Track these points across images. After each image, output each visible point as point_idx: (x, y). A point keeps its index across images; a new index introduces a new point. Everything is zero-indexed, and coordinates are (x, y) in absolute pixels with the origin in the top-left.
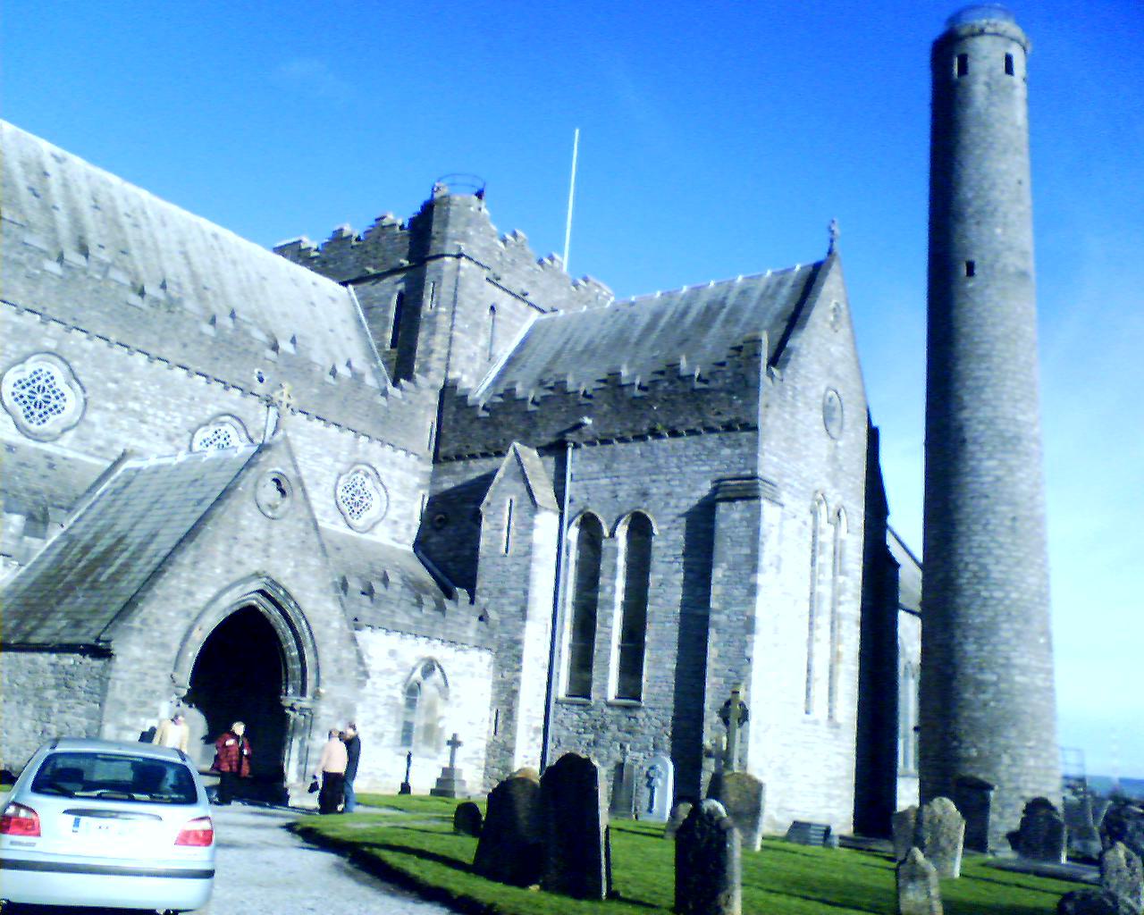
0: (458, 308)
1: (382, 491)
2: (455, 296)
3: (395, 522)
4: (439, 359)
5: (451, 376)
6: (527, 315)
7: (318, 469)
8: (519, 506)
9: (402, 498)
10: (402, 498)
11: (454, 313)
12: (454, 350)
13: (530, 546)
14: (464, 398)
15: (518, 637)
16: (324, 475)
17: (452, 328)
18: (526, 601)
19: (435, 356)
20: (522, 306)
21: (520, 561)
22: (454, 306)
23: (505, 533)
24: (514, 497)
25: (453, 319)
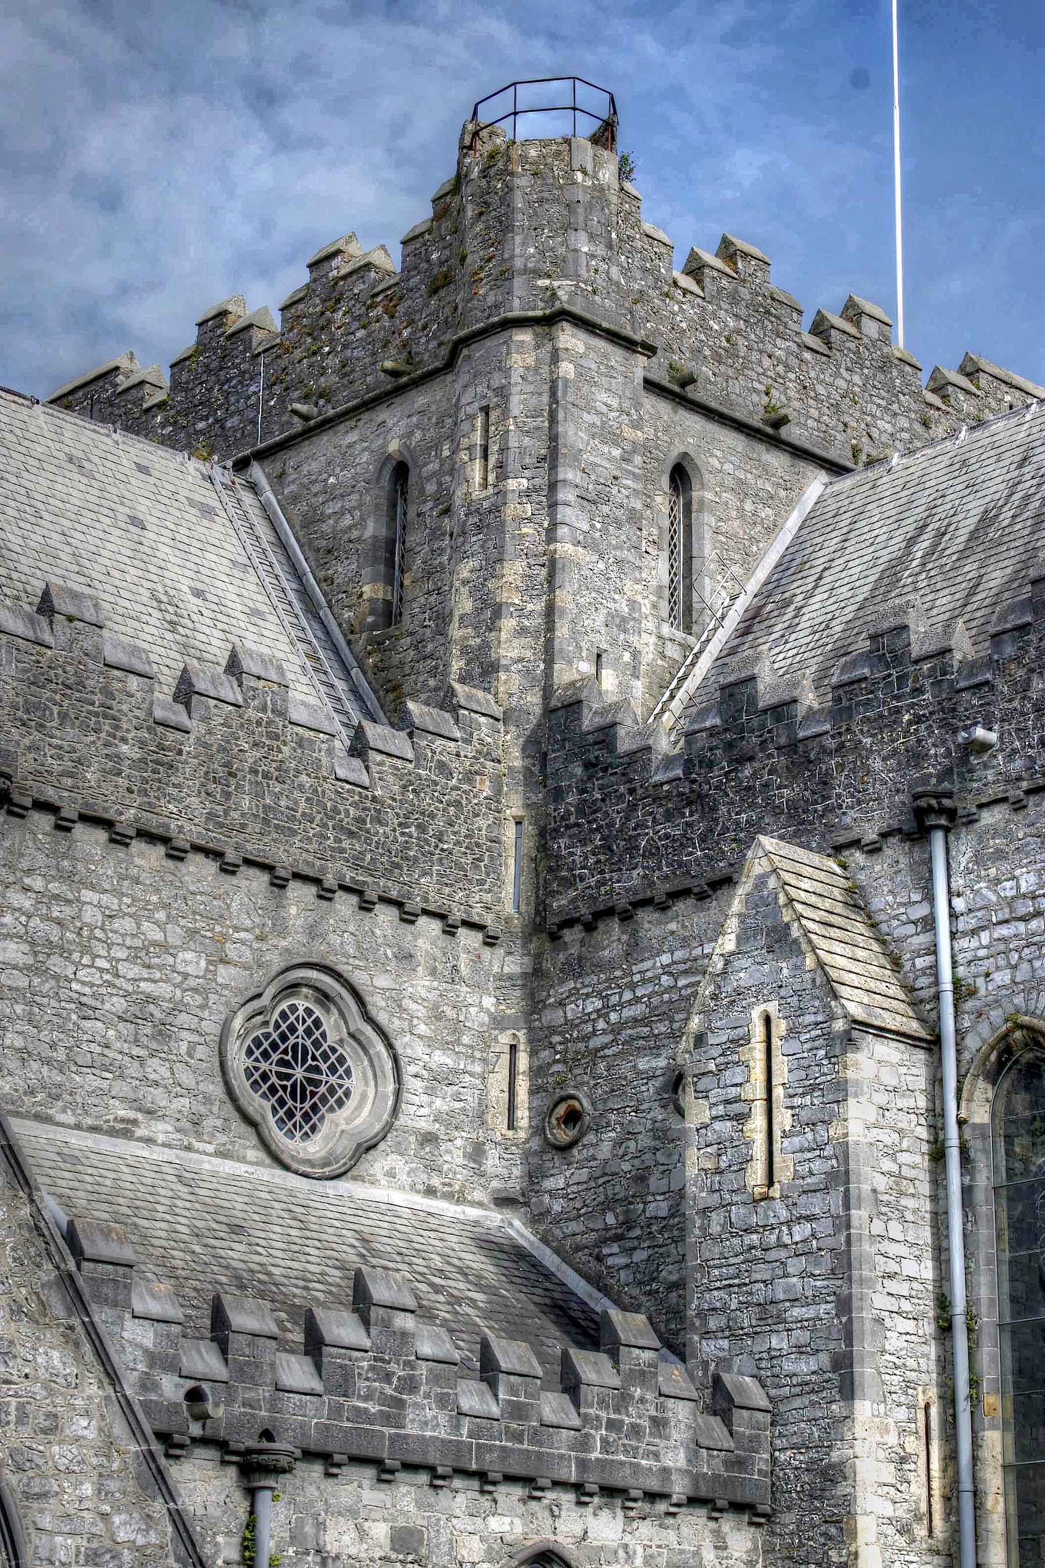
0: (567, 473)
1: (380, 1047)
2: (553, 438)
3: (429, 1139)
4: (522, 631)
5: (564, 674)
6: (794, 489)
7: (163, 990)
8: (793, 1032)
9: (441, 1059)
10: (441, 1059)
11: (553, 486)
12: (564, 598)
13: (843, 1152)
14: (606, 734)
15: (835, 1456)
16: (178, 1008)
17: (551, 535)
18: (848, 1335)
19: (508, 624)
20: (777, 461)
21: (815, 1205)
22: (553, 468)
23: (758, 1122)
24: (772, 1007)
25: (553, 505)
